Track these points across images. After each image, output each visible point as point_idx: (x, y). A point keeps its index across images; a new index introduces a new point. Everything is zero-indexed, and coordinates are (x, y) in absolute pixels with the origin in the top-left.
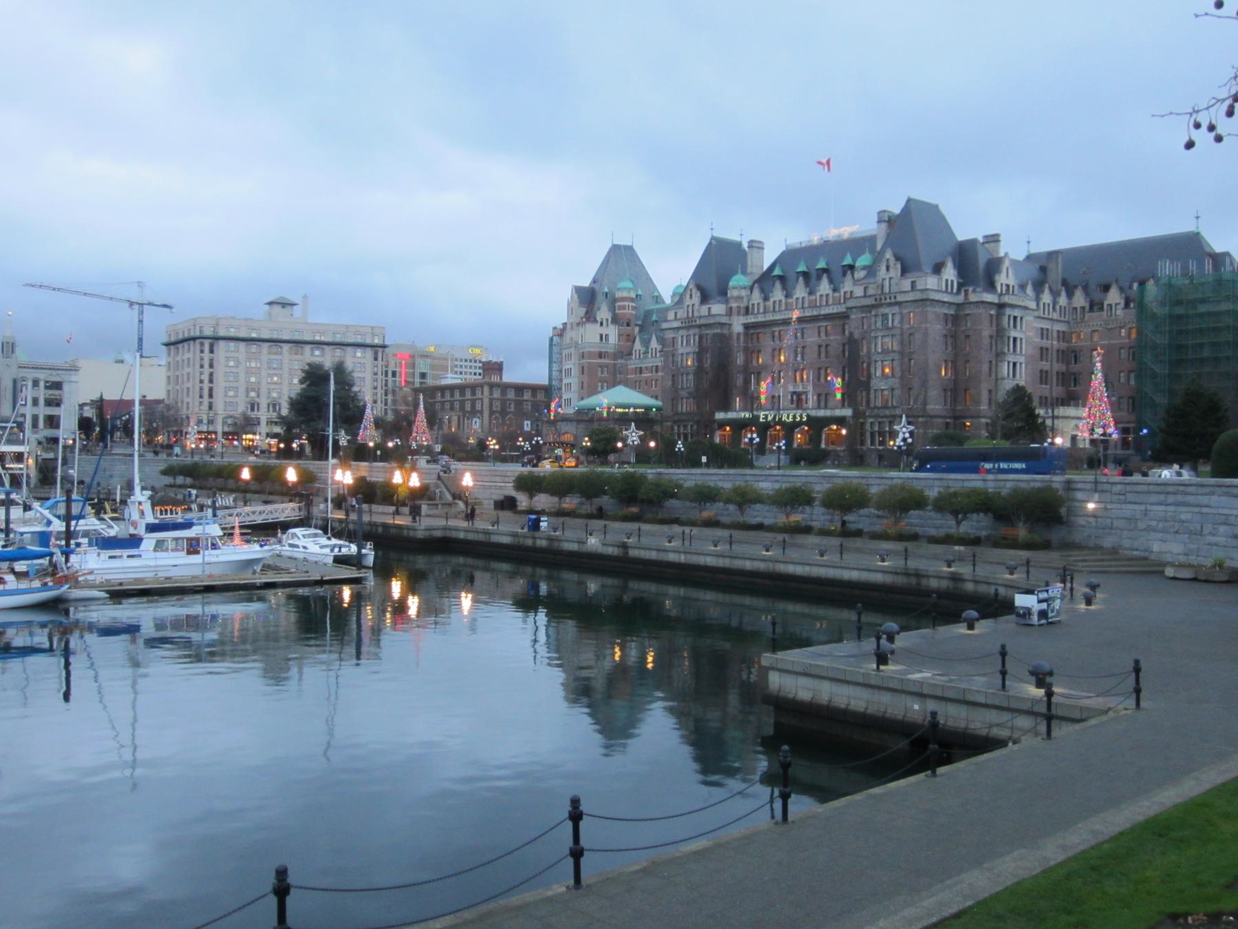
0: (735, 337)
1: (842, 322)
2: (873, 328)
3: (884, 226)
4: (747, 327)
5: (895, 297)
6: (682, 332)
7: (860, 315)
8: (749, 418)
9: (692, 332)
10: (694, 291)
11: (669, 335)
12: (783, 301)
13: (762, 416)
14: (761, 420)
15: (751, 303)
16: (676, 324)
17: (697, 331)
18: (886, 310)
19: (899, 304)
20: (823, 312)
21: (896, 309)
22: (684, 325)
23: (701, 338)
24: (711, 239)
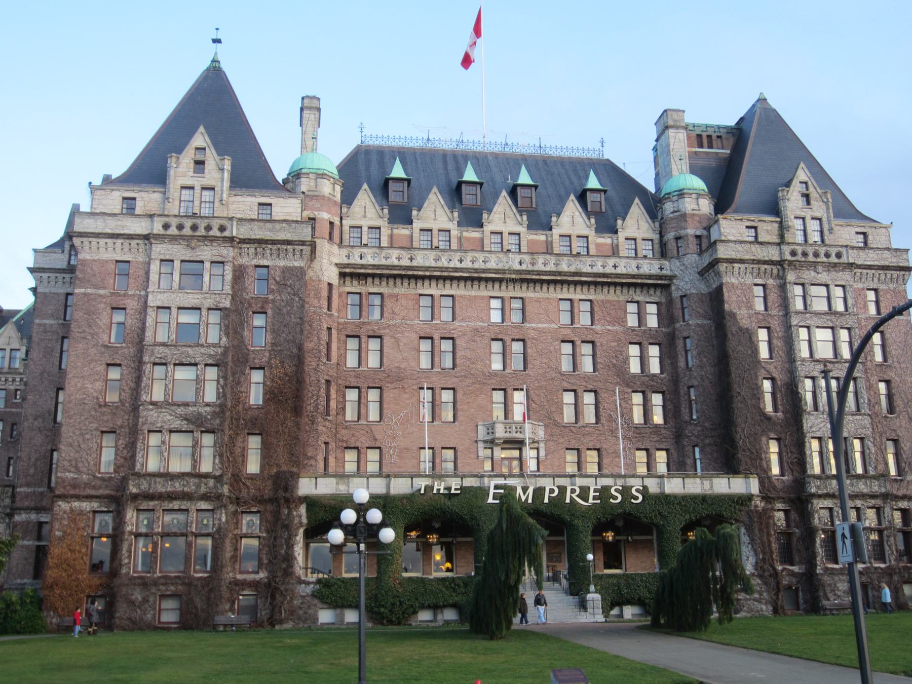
0: (325, 293)
1: (622, 298)
2: (792, 309)
3: (682, 135)
4: (347, 274)
5: (839, 255)
6: (160, 250)
7: (749, 280)
8: (450, 496)
9: (207, 253)
10: (211, 158)
11: (110, 252)
12: (455, 233)
13: (492, 491)
14: (490, 500)
15: (347, 223)
16: (138, 227)
17: (228, 252)
18: (824, 277)
19: (851, 266)
20: (586, 269)
21: (845, 277)
22: (173, 231)
23: (239, 274)
24: (214, 61)
